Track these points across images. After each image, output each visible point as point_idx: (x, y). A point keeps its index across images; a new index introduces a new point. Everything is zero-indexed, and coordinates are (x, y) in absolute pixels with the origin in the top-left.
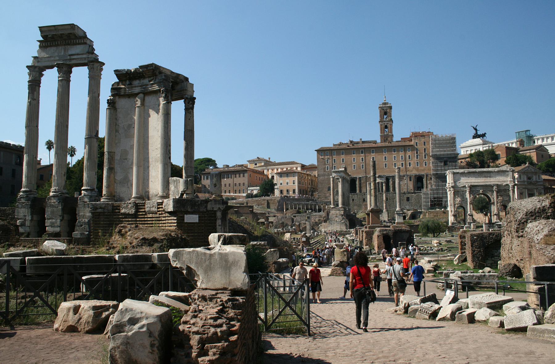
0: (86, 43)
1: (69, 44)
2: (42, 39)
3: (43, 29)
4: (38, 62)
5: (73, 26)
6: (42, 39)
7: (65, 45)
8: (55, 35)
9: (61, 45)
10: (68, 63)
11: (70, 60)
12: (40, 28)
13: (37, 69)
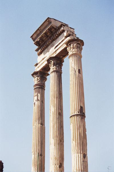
0: (64, 31)
1: (54, 40)
2: (37, 47)
3: (34, 37)
4: (38, 67)
5: (49, 20)
6: (37, 47)
7: (52, 42)
8: (42, 36)
9: (50, 44)
10: (54, 55)
11: (56, 51)
12: (31, 37)
13: (39, 74)
